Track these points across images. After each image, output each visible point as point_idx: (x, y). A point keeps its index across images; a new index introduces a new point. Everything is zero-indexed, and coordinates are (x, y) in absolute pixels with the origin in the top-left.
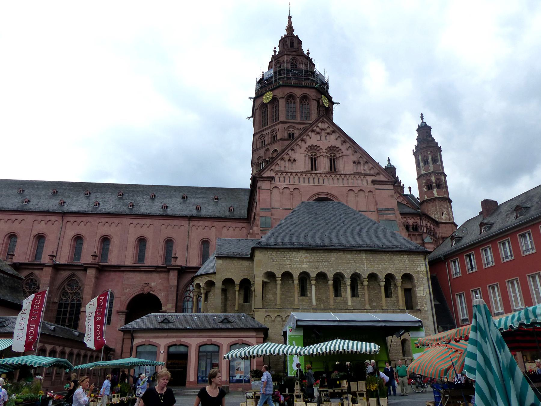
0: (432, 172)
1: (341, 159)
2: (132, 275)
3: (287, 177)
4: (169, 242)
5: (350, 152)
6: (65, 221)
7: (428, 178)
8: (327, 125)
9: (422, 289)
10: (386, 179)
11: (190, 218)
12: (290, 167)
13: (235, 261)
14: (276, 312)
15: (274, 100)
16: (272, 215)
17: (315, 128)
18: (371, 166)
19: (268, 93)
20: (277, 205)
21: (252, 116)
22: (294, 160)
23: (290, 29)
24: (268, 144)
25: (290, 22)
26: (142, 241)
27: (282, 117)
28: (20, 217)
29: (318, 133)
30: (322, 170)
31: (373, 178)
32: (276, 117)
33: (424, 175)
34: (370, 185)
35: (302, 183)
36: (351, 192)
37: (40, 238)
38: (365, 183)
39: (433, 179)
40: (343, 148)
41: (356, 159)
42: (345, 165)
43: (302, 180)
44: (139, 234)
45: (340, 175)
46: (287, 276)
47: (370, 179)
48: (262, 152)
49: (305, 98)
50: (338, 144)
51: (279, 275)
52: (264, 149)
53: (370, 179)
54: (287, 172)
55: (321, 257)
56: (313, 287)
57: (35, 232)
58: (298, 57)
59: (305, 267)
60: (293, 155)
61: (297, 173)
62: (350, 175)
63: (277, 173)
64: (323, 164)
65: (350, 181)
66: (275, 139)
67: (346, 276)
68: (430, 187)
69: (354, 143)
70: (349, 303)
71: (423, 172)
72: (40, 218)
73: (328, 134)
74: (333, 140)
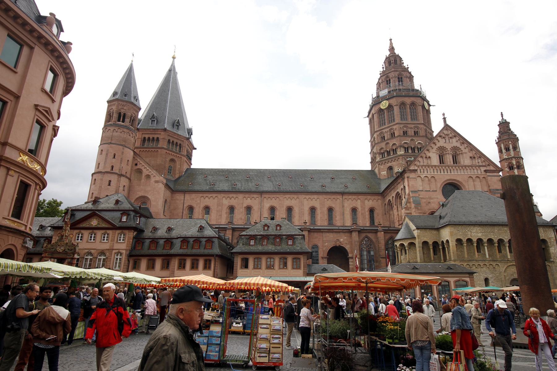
0: (513, 157)
1: (461, 155)
2: (328, 234)
3: (425, 169)
4: (330, 210)
5: (467, 150)
6: (263, 197)
7: (510, 161)
8: (450, 132)
9: (553, 248)
10: (495, 169)
11: (343, 194)
12: (426, 162)
13: (428, 230)
14: (466, 262)
15: (390, 107)
16: (419, 195)
17: (441, 134)
18: (483, 159)
19: (385, 102)
20: (421, 189)
21: (368, 117)
22: (429, 157)
23: (392, 49)
24: (388, 140)
25: (391, 43)
26: (313, 210)
27: (397, 119)
28: (235, 196)
29: (444, 138)
30: (449, 163)
31: (485, 168)
32: (392, 119)
33: (506, 159)
34: (483, 173)
35: (436, 173)
36: (471, 178)
37: (249, 209)
38: (479, 172)
39: (514, 162)
40: (462, 147)
41: (471, 155)
42: (465, 160)
43: (435, 171)
44: (311, 205)
45: (462, 167)
46: (469, 241)
47: (483, 169)
48: (383, 145)
49: (413, 104)
50: (458, 145)
51: (464, 240)
52: (385, 143)
53: (483, 169)
54: (425, 166)
55: (489, 229)
56: (486, 247)
57: (245, 205)
58: (403, 73)
59: (480, 235)
60: (428, 154)
61: (432, 166)
62: (469, 166)
63: (418, 166)
64: (449, 159)
65: (469, 170)
66: (393, 135)
67: (506, 241)
68: (511, 168)
69: (470, 144)
70: (509, 257)
71: (505, 157)
72: (247, 196)
73: (451, 138)
74: (455, 143)
